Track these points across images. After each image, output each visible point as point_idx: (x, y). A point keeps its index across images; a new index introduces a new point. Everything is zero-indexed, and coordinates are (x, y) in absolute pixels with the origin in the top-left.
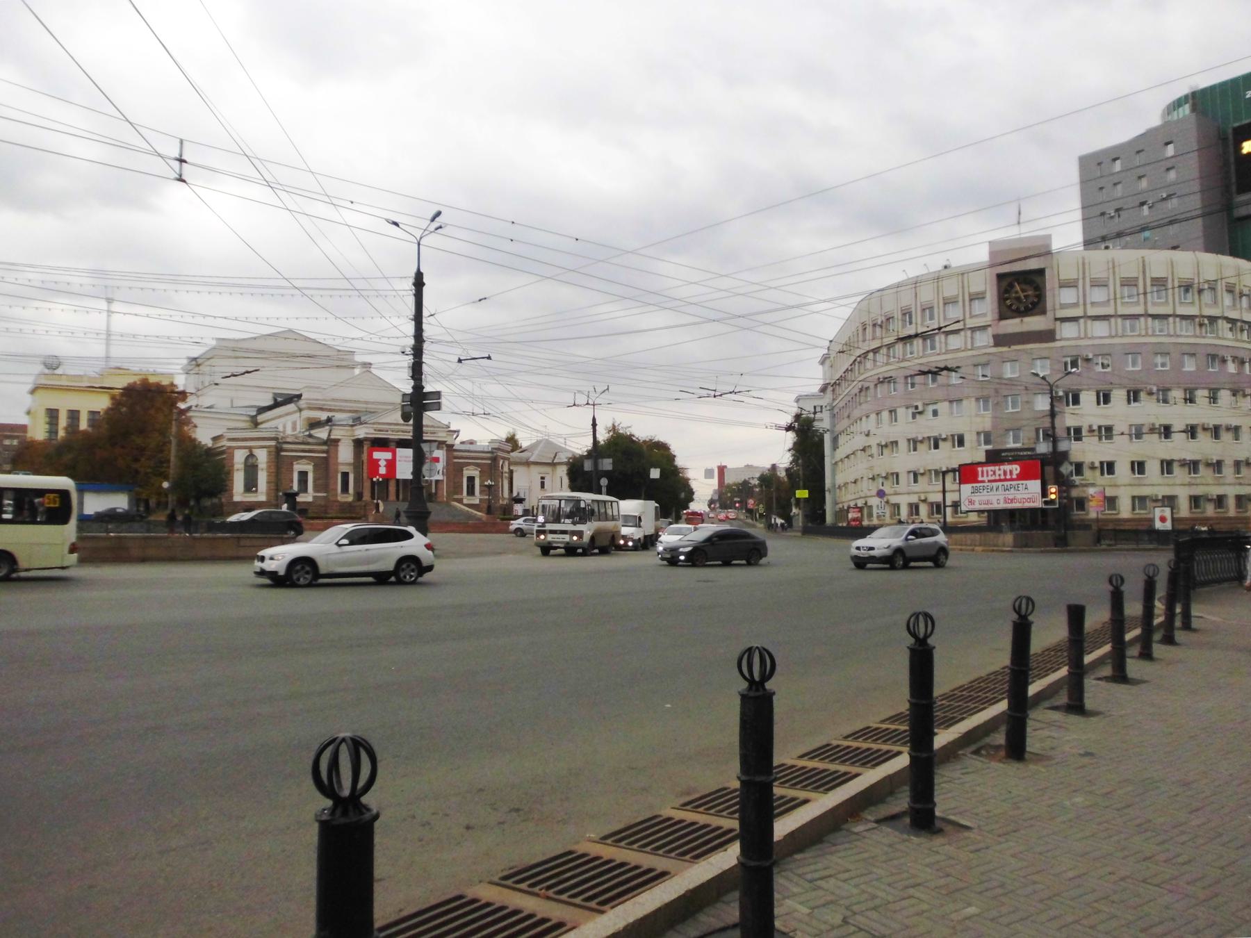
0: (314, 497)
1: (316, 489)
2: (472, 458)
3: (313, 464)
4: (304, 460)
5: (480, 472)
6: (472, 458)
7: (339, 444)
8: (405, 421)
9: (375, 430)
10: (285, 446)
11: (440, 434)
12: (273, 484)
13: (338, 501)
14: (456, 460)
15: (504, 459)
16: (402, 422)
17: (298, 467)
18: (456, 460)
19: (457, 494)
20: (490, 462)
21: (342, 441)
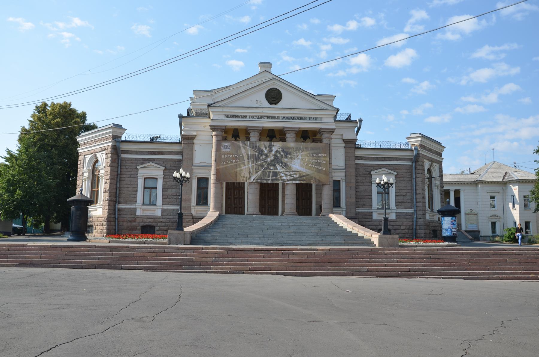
0: (163, 211)
1: (164, 203)
2: (384, 159)
3: (163, 168)
4: (151, 163)
5: (396, 177)
6: (384, 159)
7: (195, 141)
8: (271, 104)
9: (227, 116)
10: (124, 147)
11: (325, 120)
12: (107, 194)
13: (192, 216)
14: (358, 162)
15: (432, 161)
16: (266, 104)
17: (143, 172)
18: (358, 162)
19: (363, 206)
20: (409, 163)
21: (197, 138)
